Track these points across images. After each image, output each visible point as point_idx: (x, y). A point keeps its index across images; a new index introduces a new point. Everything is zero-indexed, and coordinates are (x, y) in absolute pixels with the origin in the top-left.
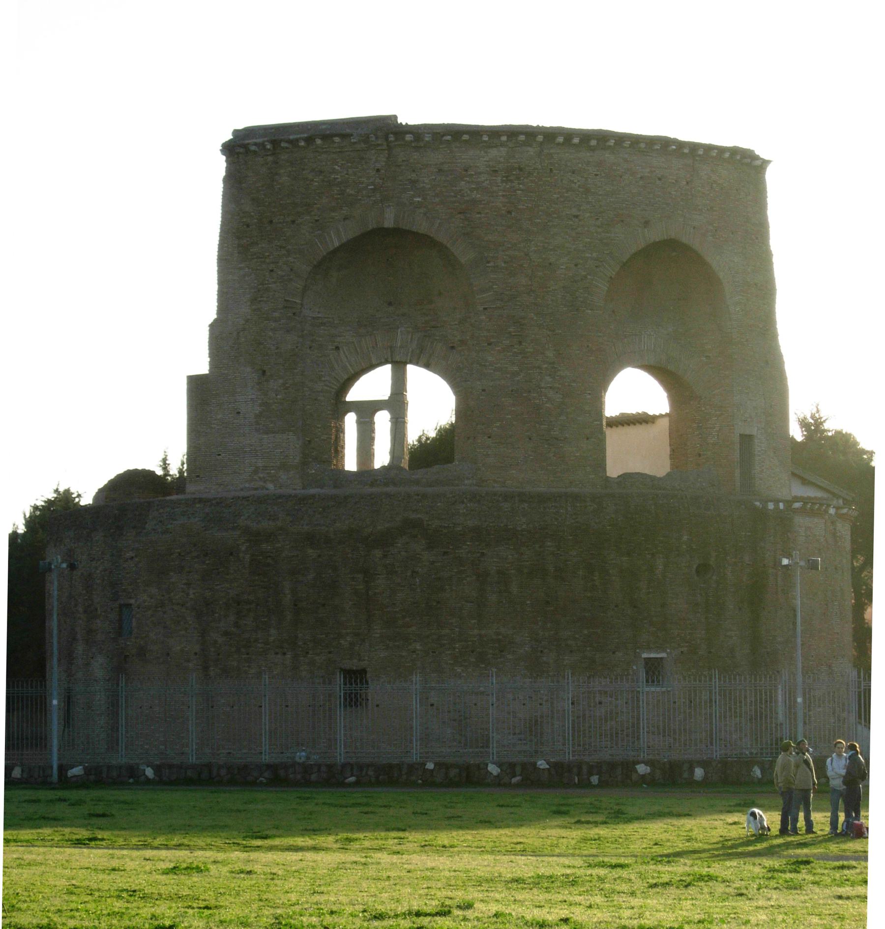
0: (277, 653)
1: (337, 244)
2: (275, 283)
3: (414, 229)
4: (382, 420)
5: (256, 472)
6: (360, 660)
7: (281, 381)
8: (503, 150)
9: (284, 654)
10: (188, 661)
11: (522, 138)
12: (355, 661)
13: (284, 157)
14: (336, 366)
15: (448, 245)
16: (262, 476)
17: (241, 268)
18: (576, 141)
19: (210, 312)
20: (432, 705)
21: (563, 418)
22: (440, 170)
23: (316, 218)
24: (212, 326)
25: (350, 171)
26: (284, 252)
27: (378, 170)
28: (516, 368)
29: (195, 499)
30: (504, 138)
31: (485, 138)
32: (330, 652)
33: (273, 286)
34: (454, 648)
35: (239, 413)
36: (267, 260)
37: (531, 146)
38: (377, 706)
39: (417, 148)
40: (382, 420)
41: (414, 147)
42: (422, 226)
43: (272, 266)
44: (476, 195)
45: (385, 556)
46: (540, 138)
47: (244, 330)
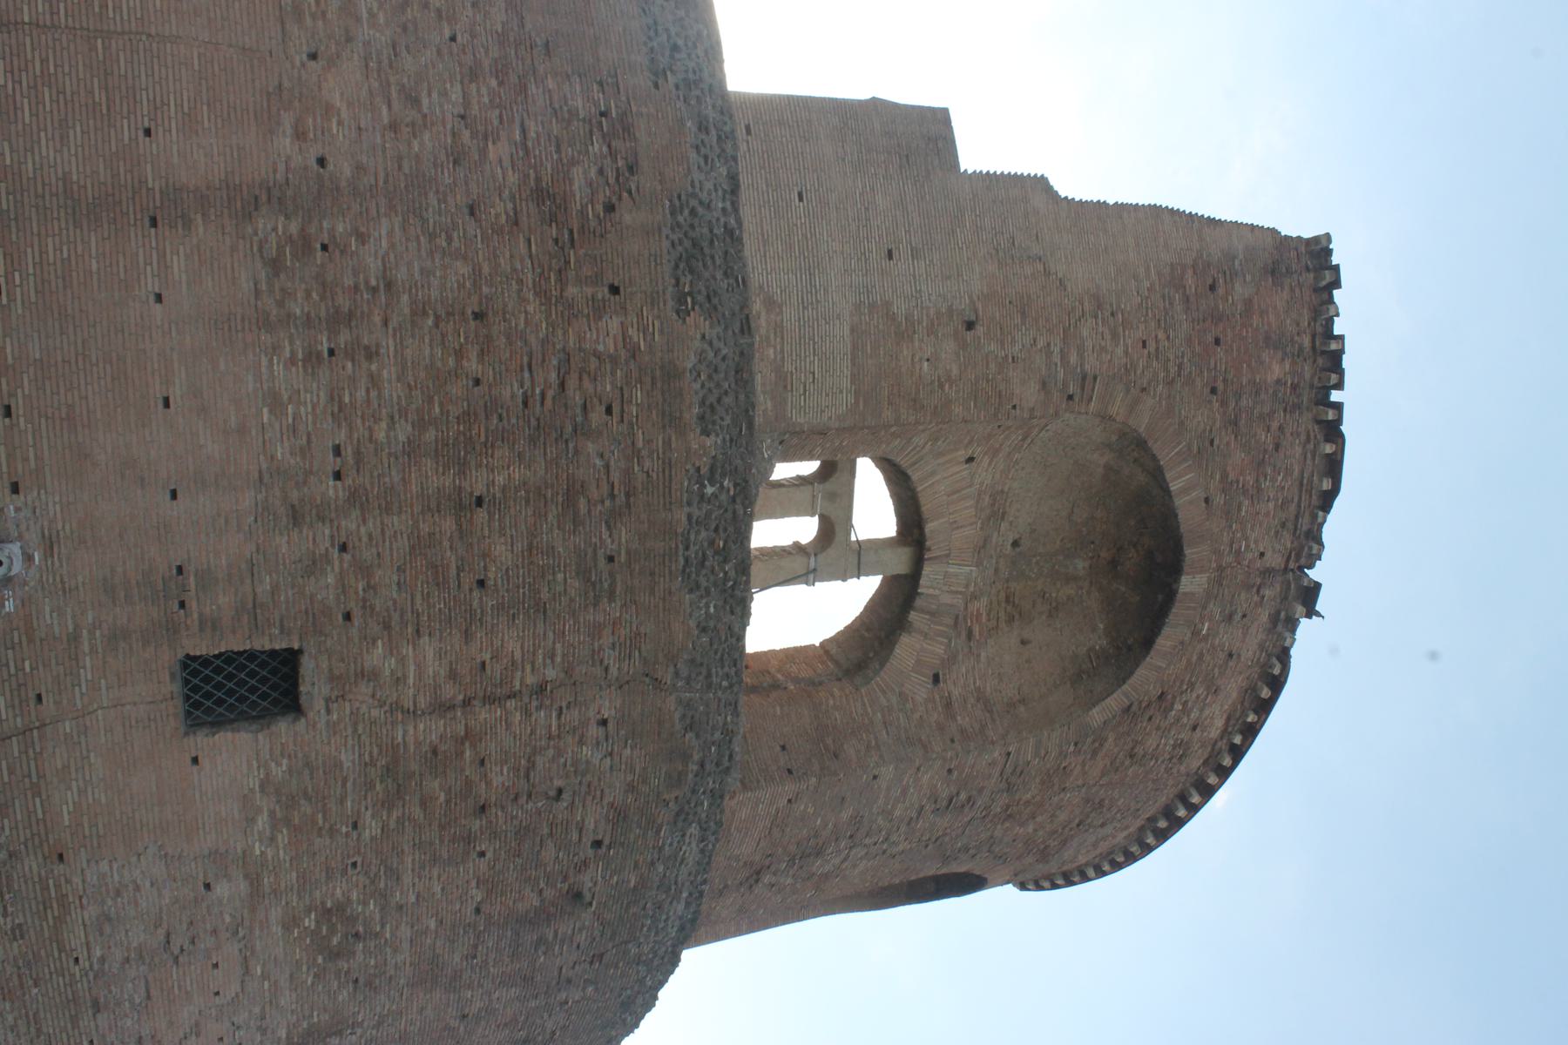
0: (337, 451)
1: (1174, 487)
2: (1126, 353)
3: (1166, 631)
4: (804, 529)
5: (770, 303)
6: (328, 700)
7: (955, 371)
8: (1214, 733)
9: (338, 476)
10: (300, 135)
11: (1227, 762)
12: (325, 690)
13: (1307, 371)
14: (941, 461)
15: (1126, 687)
16: (763, 322)
17: (1148, 269)
18: (1182, 813)
19: (1072, 185)
20: (207, 886)
21: (789, 881)
22: (1231, 655)
23: (1216, 442)
24: (1041, 183)
25: (1271, 505)
26: (1173, 370)
27: (1262, 554)
28: (897, 813)
29: (735, 159)
30: (1238, 740)
31: (1251, 718)
32: (348, 617)
33: (1120, 351)
34: (365, 904)
35: (890, 255)
36: (1161, 335)
37: (1206, 762)
38: (195, 760)
39: (1274, 619)
40: (804, 529)
41: (1278, 613)
42: (1164, 642)
43: (1152, 346)
44: (1178, 707)
45: (604, 722)
46: (1212, 780)
47: (1047, 273)
